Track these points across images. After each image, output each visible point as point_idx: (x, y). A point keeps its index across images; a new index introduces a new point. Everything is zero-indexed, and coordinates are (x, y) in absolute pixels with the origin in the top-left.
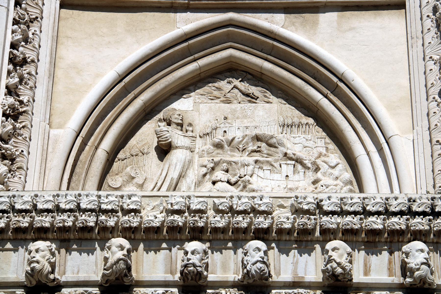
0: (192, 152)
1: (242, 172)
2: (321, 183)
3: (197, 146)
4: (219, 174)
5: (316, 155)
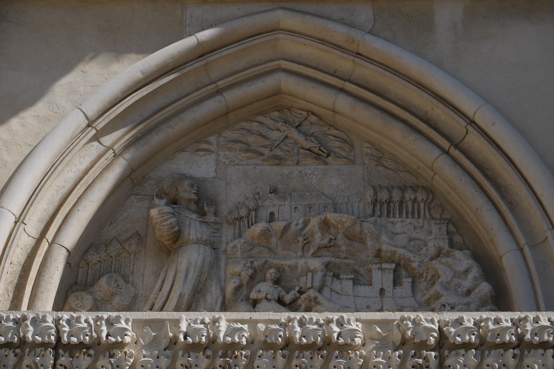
0: (214, 249)
2: (442, 300)
3: (224, 239)
5: (432, 251)
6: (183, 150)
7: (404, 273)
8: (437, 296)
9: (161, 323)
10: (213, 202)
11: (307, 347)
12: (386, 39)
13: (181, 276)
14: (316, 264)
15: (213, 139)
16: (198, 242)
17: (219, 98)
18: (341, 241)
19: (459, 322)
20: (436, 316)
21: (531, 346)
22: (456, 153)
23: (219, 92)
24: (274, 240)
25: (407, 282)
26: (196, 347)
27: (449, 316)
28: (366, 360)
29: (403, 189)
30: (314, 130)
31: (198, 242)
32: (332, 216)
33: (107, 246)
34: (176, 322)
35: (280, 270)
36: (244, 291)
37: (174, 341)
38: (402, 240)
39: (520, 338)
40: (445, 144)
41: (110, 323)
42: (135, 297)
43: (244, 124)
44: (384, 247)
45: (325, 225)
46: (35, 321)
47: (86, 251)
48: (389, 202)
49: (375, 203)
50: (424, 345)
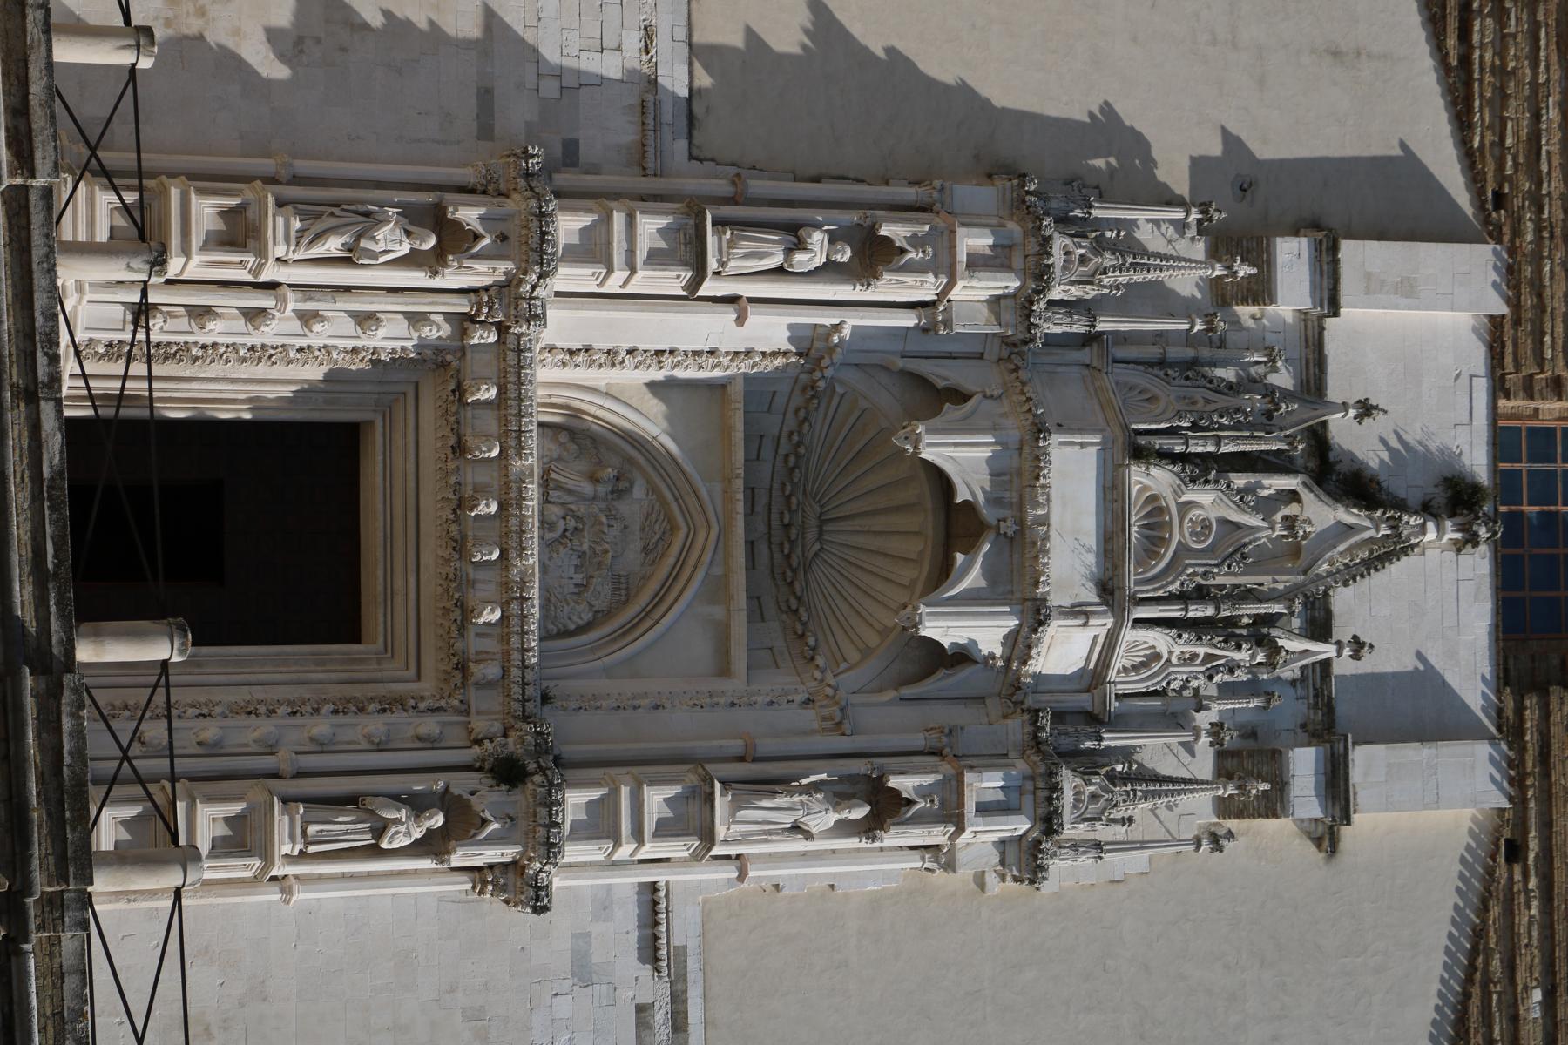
1: (576, 542)
2: (566, 607)
4: (572, 523)
6: (648, 483)
7: (582, 589)
8: (568, 604)
9: (533, 476)
10: (619, 498)
11: (521, 540)
12: (703, 581)
13: (577, 483)
14: (585, 547)
15: (654, 497)
16: (596, 491)
17: (673, 499)
18: (597, 560)
19: (533, 606)
20: (536, 596)
21: (522, 638)
22: (643, 614)
23: (676, 500)
24: (598, 527)
25: (577, 590)
26: (521, 492)
27: (537, 602)
28: (516, 566)
29: (627, 589)
30: (660, 546)
31: (596, 491)
32: (610, 555)
33: (595, 448)
34: (532, 483)
35: (582, 530)
36: (571, 513)
37: (524, 482)
38: (599, 588)
39: (527, 633)
40: (647, 610)
41: (531, 454)
42: (568, 462)
43: (662, 513)
44: (595, 580)
45: (606, 552)
46: (531, 421)
47: (592, 438)
48: (619, 582)
49: (619, 576)
50: (522, 591)
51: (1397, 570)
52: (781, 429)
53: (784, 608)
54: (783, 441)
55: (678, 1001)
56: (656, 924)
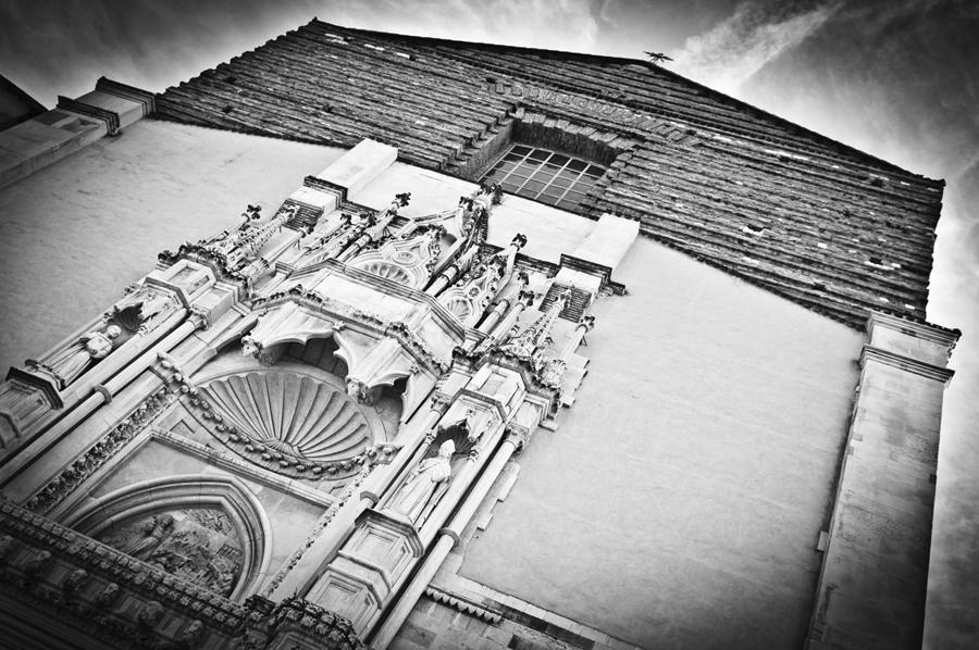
4: (164, 559)
16: (155, 537)
38: (219, 564)
51: (491, 221)
52: (211, 433)
53: (317, 477)
54: (218, 435)
55: (523, 618)
56: (455, 607)
